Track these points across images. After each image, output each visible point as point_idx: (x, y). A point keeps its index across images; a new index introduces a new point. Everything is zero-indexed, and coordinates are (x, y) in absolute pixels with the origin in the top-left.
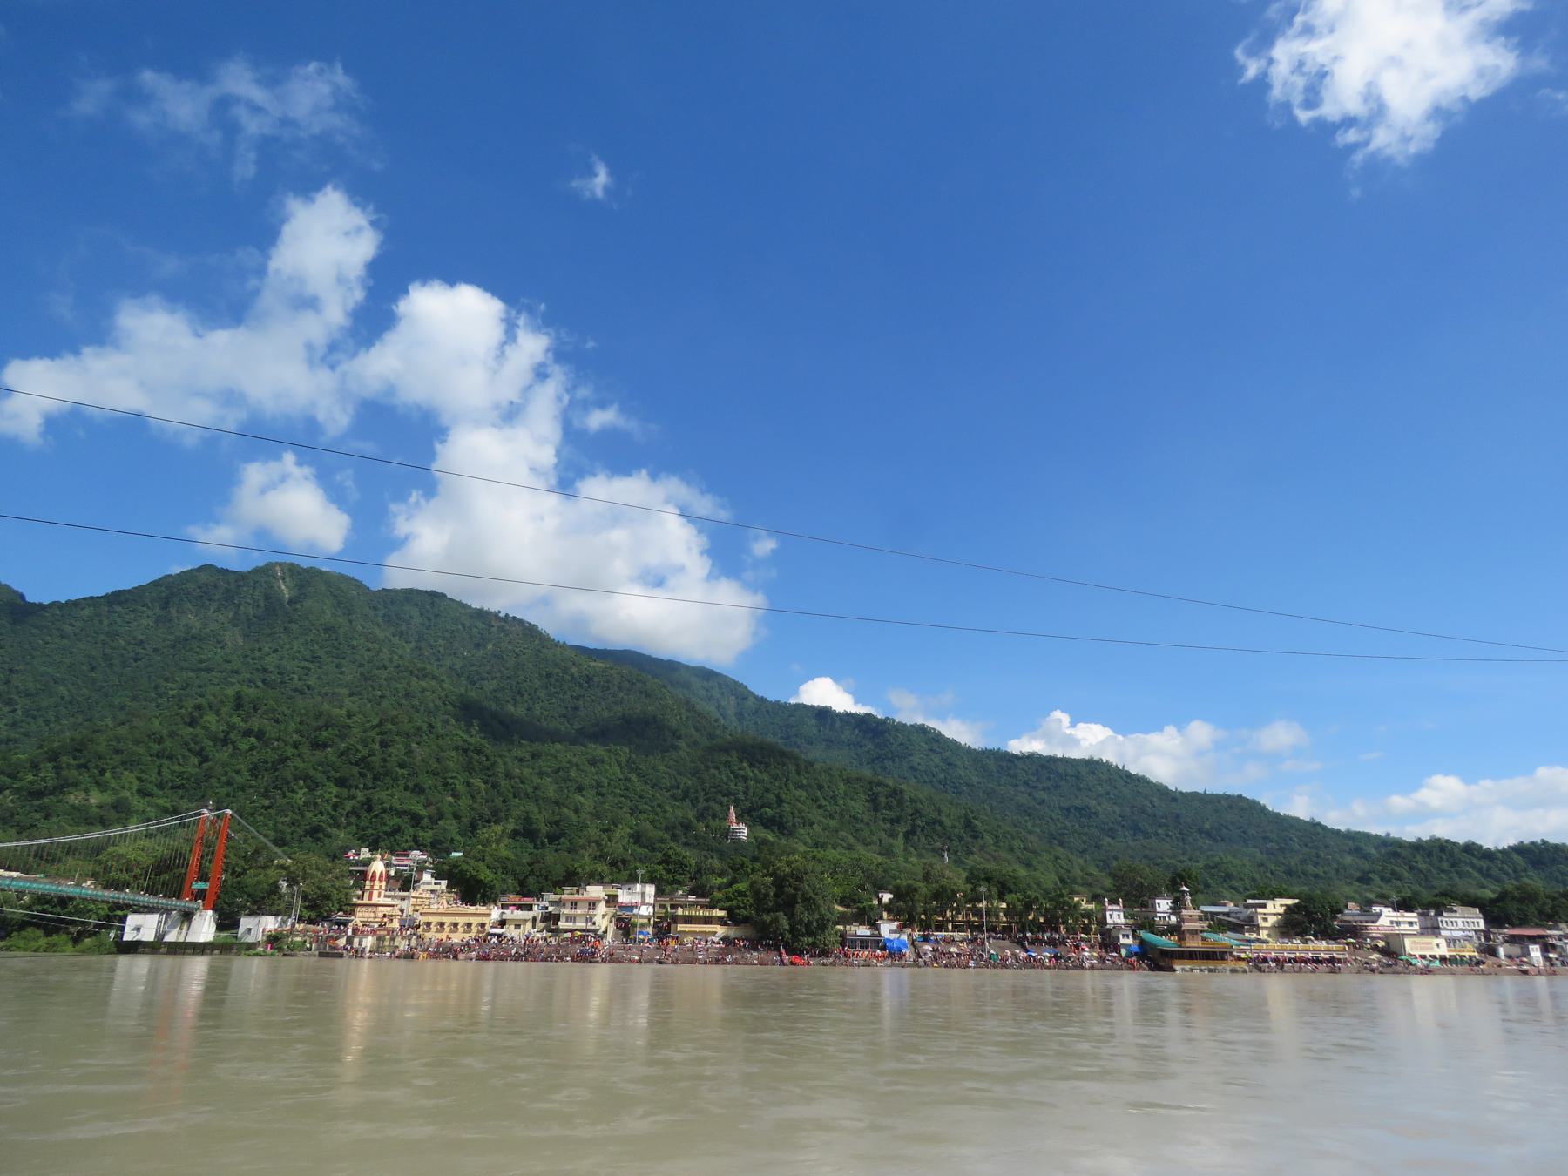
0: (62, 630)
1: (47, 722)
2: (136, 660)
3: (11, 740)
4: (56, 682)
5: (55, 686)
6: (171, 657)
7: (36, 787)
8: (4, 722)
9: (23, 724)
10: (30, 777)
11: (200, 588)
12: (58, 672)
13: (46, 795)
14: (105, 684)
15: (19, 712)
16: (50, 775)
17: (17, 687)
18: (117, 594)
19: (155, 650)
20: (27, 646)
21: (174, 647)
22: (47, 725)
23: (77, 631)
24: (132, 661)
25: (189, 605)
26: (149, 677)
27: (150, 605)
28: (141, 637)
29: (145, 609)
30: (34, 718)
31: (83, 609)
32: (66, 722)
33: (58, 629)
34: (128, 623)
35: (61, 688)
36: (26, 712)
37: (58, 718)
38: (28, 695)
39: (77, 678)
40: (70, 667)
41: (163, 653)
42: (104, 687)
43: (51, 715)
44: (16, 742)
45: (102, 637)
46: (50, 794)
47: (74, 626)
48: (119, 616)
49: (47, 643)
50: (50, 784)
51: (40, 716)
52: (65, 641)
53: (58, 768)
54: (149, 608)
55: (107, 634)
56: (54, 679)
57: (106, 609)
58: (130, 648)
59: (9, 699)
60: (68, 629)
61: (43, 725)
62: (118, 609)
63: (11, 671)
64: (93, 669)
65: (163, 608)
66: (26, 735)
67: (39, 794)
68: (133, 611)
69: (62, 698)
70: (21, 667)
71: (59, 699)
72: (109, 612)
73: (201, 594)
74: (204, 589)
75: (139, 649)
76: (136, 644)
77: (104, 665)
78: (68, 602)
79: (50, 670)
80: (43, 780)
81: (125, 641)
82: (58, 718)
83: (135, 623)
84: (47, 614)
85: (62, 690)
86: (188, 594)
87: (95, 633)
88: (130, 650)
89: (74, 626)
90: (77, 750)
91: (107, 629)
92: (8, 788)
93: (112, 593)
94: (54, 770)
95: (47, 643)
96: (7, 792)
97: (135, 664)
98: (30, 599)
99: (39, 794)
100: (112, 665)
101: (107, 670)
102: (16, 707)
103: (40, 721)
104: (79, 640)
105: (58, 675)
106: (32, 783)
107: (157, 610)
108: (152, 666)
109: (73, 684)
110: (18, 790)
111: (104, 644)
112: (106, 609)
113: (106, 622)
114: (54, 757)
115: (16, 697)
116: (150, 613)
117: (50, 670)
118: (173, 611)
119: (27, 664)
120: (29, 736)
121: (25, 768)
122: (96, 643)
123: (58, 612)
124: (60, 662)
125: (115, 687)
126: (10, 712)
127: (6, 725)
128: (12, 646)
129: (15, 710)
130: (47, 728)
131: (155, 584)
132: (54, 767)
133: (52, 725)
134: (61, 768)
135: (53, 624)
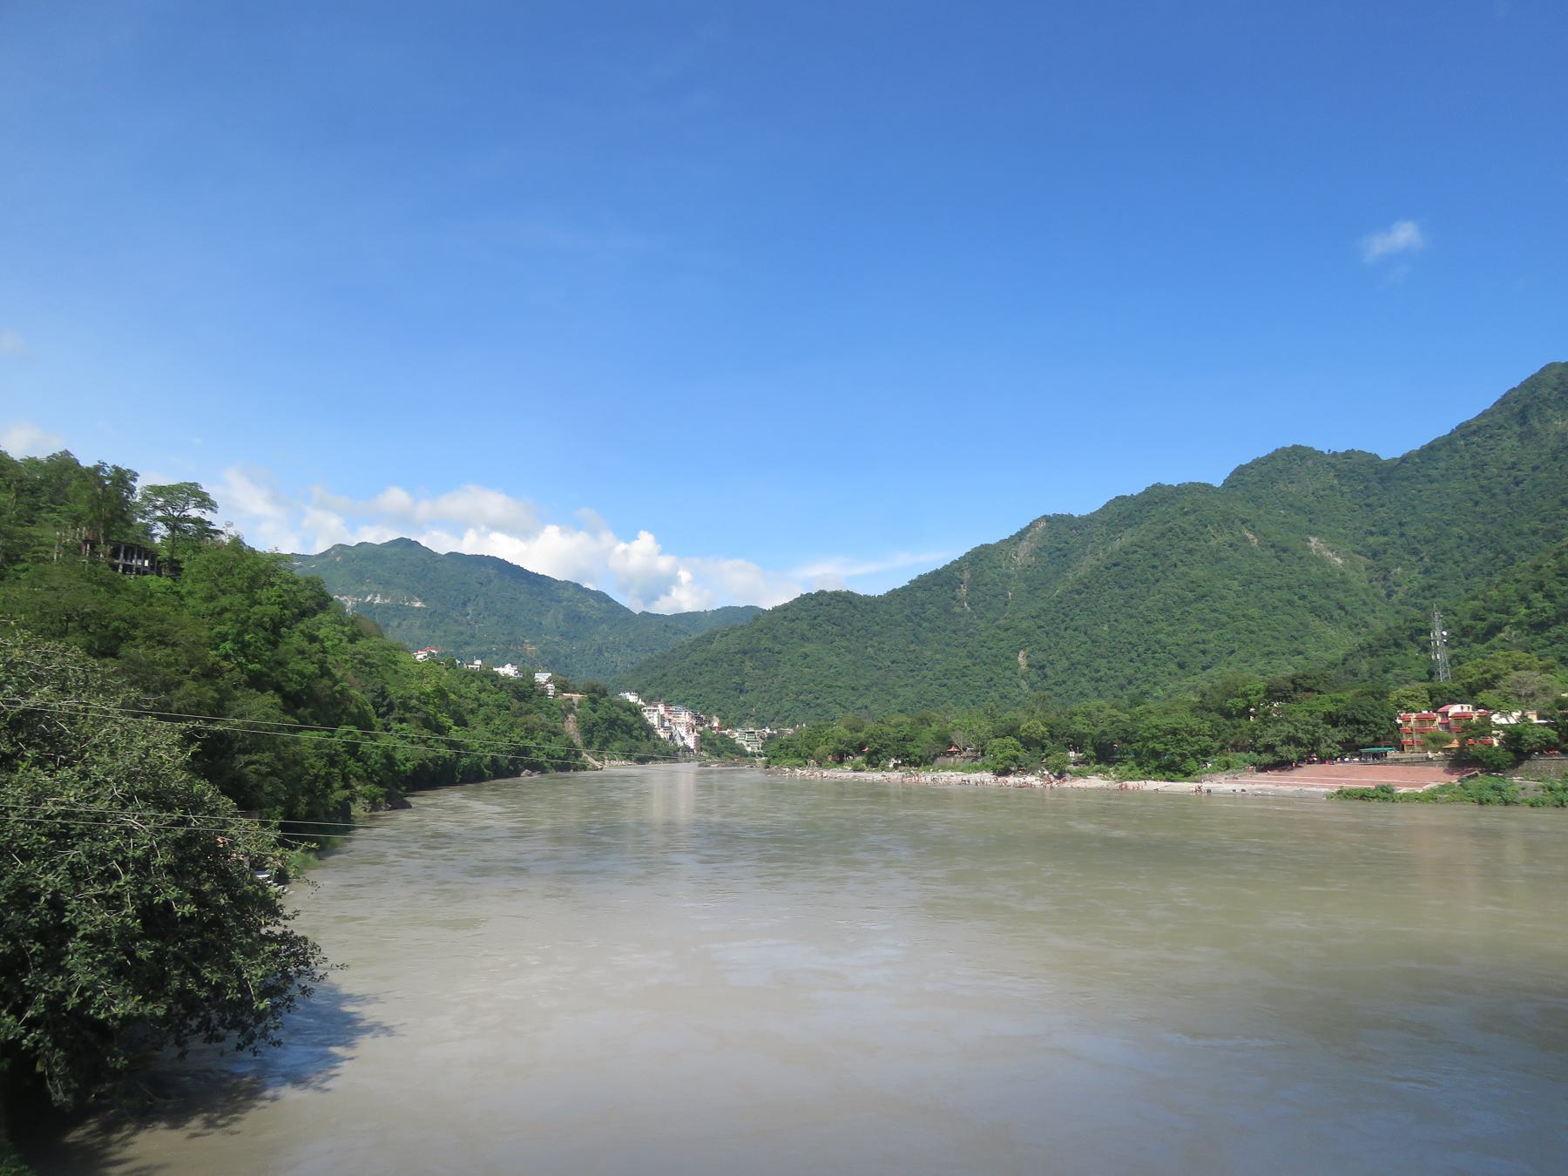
0: (1429, 476)
1: (1456, 563)
2: (1517, 484)
3: (1432, 586)
4: (1447, 525)
5: (1448, 528)
6: (1557, 470)
7: (1535, 619)
8: (1417, 570)
9: (1436, 569)
10: (1524, 611)
11: (1556, 389)
12: (1446, 514)
13: (1551, 626)
14: (1496, 516)
15: (1426, 559)
16: (1545, 604)
17: (1415, 537)
18: (1467, 425)
19: (1535, 469)
20: (1403, 499)
21: (1555, 459)
22: (1458, 566)
23: (1443, 472)
24: (1512, 486)
25: (1550, 411)
26: (1543, 497)
27: (1506, 425)
28: (1513, 460)
29: (1502, 431)
30: (1442, 561)
31: (1439, 450)
32: (1474, 560)
33: (1423, 476)
34: (1491, 449)
35: (1455, 529)
36: (1433, 558)
37: (1465, 559)
38: (1427, 542)
39: (1466, 516)
40: (1454, 507)
41: (1546, 468)
42: (1494, 519)
43: (1457, 556)
44: (1436, 588)
45: (1470, 472)
46: (1557, 622)
47: (1437, 469)
48: (1478, 446)
49: (1420, 491)
50: (1552, 613)
51: (1449, 559)
52: (1435, 485)
53: (1549, 596)
54: (1506, 428)
55: (1474, 466)
56: (1444, 522)
57: (1462, 443)
58: (1505, 473)
59: (1413, 549)
60: (1433, 473)
61: (1454, 566)
62: (1476, 439)
63: (1400, 524)
64: (1476, 504)
65: (1521, 425)
66: (1442, 579)
67: (1541, 627)
68: (1491, 437)
69: (1461, 538)
70: (1408, 519)
71: (1459, 540)
72: (1466, 446)
73: (1559, 396)
74: (1561, 388)
75: (1514, 472)
76: (1509, 469)
77: (1485, 497)
78: (1422, 449)
79: (1435, 514)
80: (1543, 610)
81: (1496, 467)
82: (1465, 559)
83: (1498, 448)
84: (1408, 465)
85: (1456, 530)
86: (1545, 400)
87: (1463, 469)
88: (1506, 475)
89: (1437, 469)
90: (1561, 575)
91: (1470, 463)
92: (1506, 624)
93: (1457, 428)
94: (1546, 600)
95: (1420, 491)
96: (1507, 628)
97: (1518, 489)
98: (1385, 457)
99: (1541, 627)
100: (1494, 495)
101: (1491, 501)
102: (1421, 555)
103: (1450, 563)
104: (1449, 480)
105: (1445, 517)
106: (1529, 616)
107: (1517, 428)
108: (1540, 484)
109: (1464, 523)
110: (1519, 624)
111: (1475, 477)
112: (1462, 443)
113: (1467, 456)
114: (1539, 587)
115: (1419, 546)
116: (1509, 433)
117: (1435, 514)
118: (1535, 423)
119: (1412, 514)
120: (1447, 580)
121: (1514, 602)
122: (1466, 478)
123: (1417, 460)
124: (1442, 505)
125: (1509, 515)
126: (1418, 560)
127: (1419, 573)
128: (1391, 502)
129: (1422, 559)
130: (1459, 569)
131: (1503, 402)
132: (1544, 597)
133: (1462, 565)
134: (1553, 596)
135: (1418, 471)
